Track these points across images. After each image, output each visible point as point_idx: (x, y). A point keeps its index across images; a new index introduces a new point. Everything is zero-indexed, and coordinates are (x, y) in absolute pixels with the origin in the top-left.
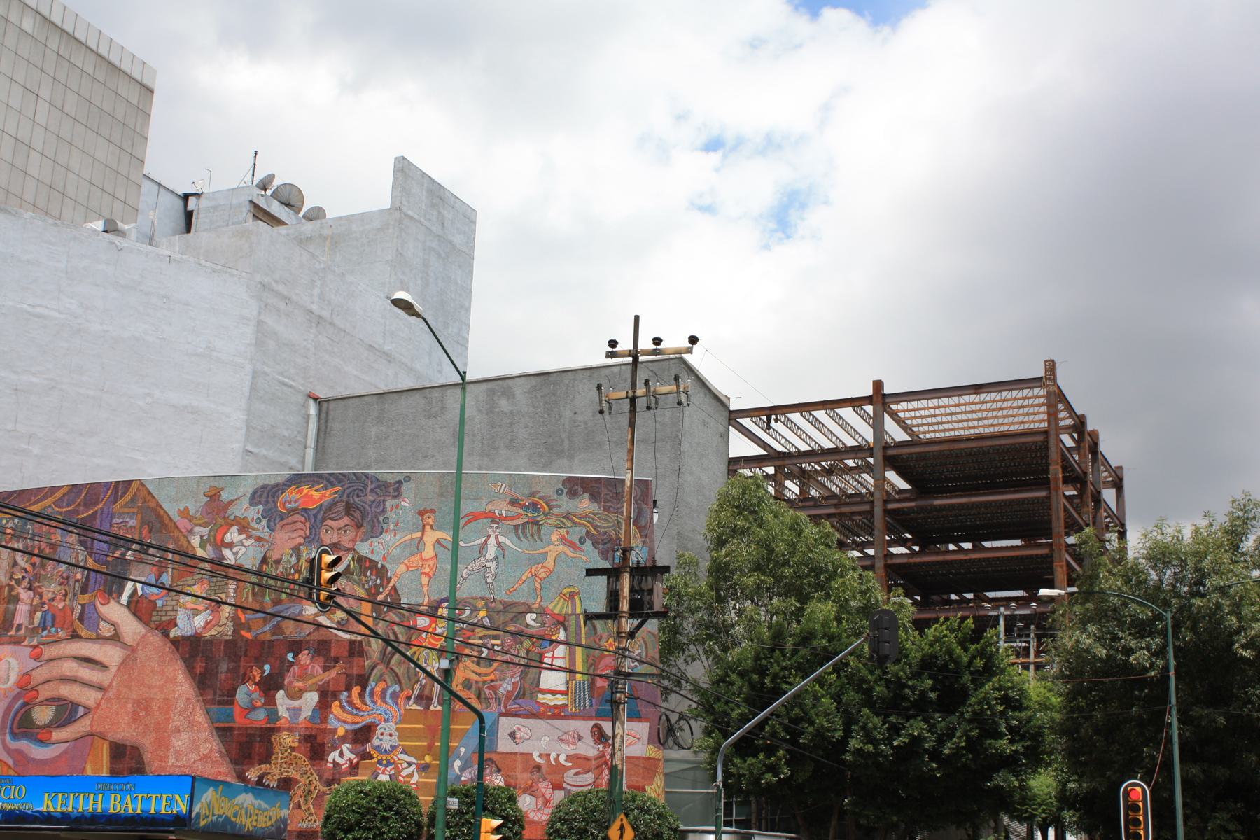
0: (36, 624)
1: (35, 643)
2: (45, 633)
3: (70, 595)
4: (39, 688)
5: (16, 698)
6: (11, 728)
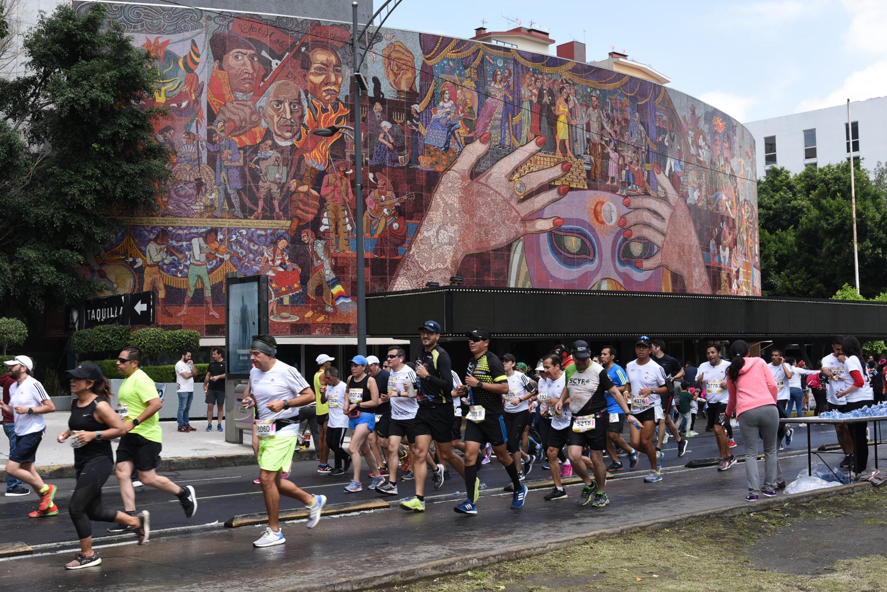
0: (624, 179)
1: (624, 194)
2: (630, 187)
3: (640, 162)
4: (632, 228)
5: (618, 234)
6: (619, 257)
